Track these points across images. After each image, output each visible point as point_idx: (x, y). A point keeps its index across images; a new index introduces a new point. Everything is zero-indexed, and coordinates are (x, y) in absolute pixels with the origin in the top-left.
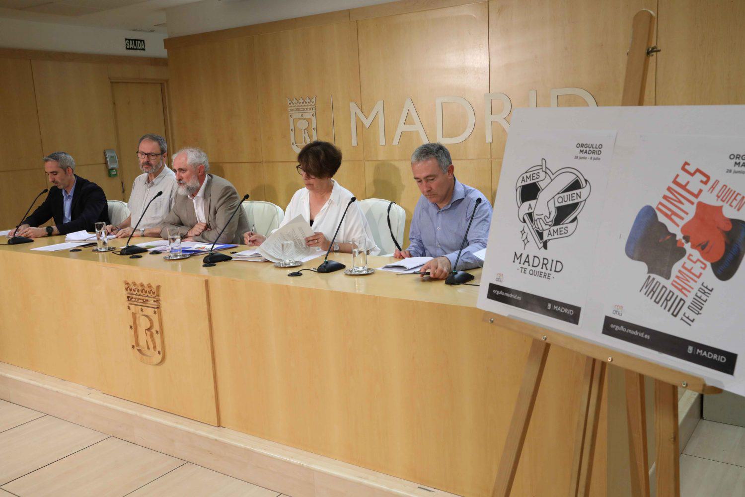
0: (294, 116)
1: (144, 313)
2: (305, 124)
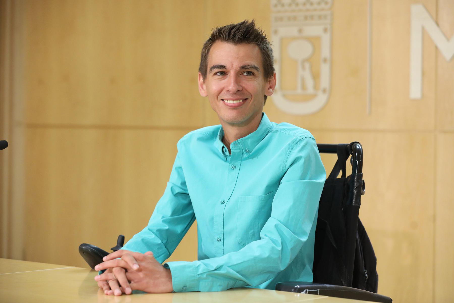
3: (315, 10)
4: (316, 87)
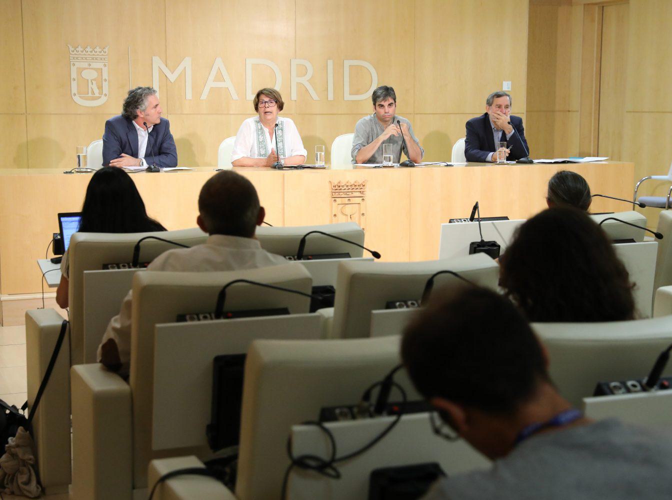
0: (78, 65)
1: (350, 203)
2: (94, 75)
3: (98, 55)
4: (101, 93)
